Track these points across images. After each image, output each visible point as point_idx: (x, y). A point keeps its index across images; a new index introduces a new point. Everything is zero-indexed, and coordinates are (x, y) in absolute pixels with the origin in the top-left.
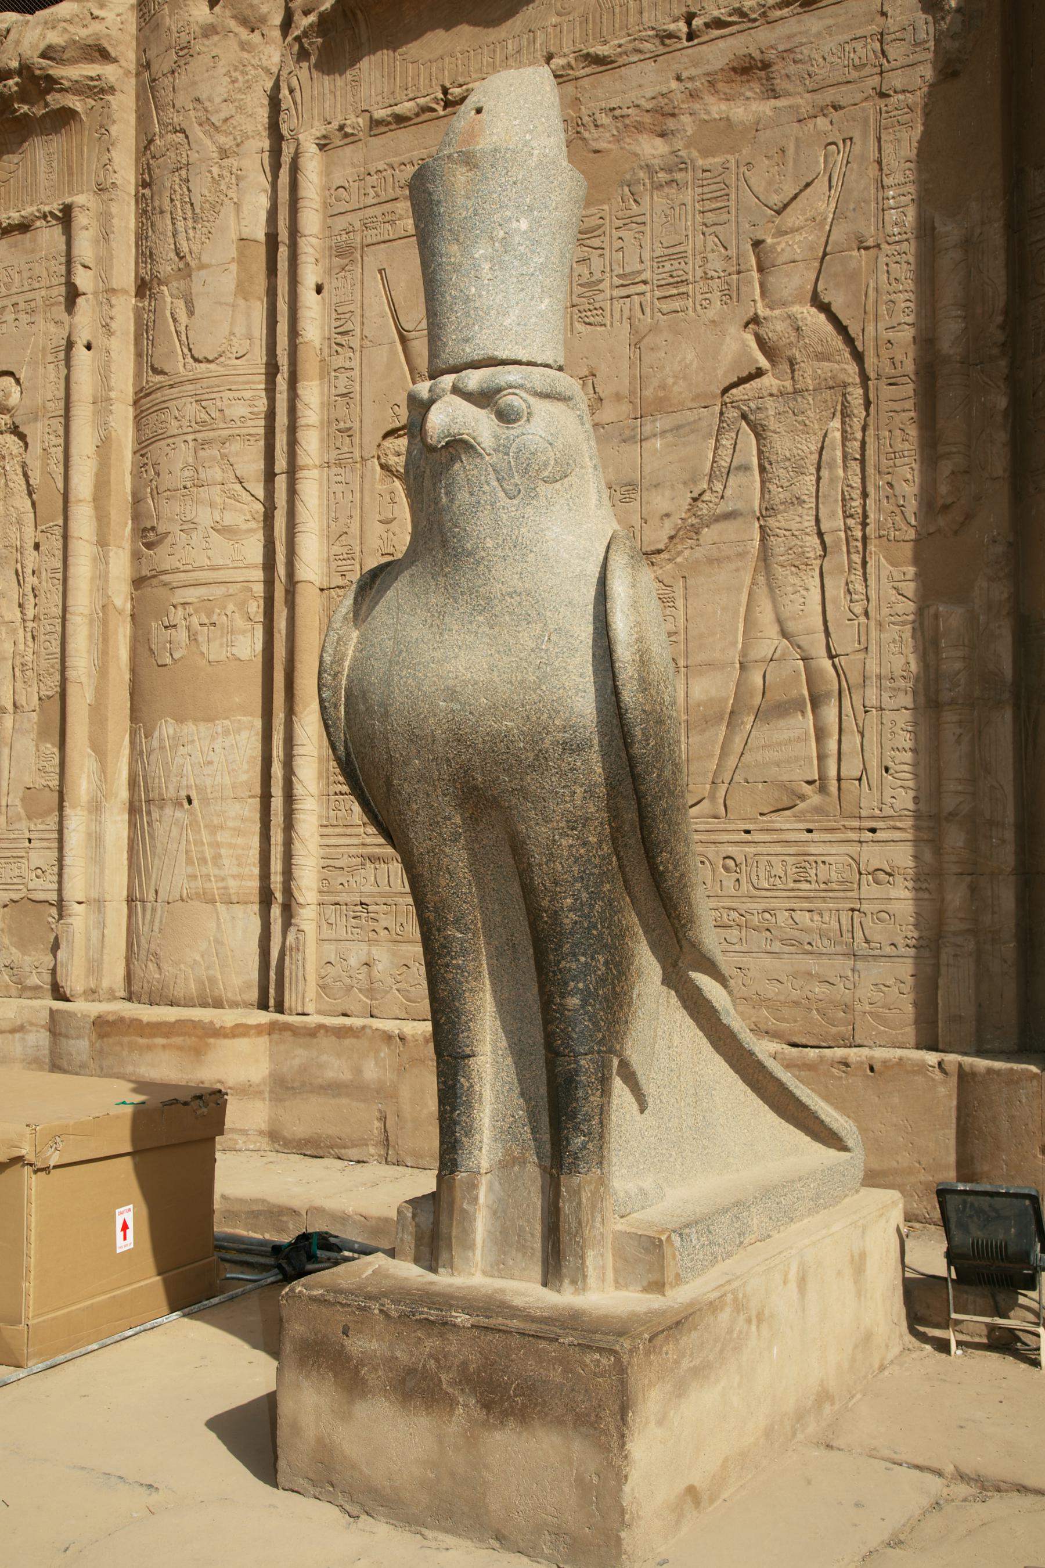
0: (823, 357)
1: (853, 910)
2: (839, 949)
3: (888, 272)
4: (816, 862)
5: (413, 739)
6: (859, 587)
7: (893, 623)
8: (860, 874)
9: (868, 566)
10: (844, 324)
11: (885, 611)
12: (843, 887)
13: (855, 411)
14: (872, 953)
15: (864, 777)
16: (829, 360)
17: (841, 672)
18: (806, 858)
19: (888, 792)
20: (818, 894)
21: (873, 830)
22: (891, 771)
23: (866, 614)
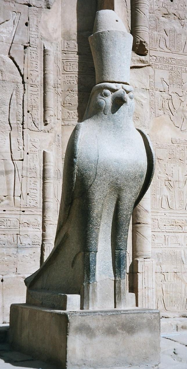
0: (12, 73)
1: (17, 234)
2: (13, 246)
3: (31, 54)
4: (7, 220)
5: (105, 170)
6: (21, 141)
7: (31, 153)
8: (20, 224)
9: (24, 136)
10: (18, 65)
11: (29, 150)
12: (14, 228)
13: (21, 91)
14: (23, 247)
15: (22, 196)
16: (13, 74)
17: (15, 165)
18: (4, 219)
19: (28, 201)
20: (7, 229)
21: (24, 211)
22: (29, 195)
23: (23, 149)
